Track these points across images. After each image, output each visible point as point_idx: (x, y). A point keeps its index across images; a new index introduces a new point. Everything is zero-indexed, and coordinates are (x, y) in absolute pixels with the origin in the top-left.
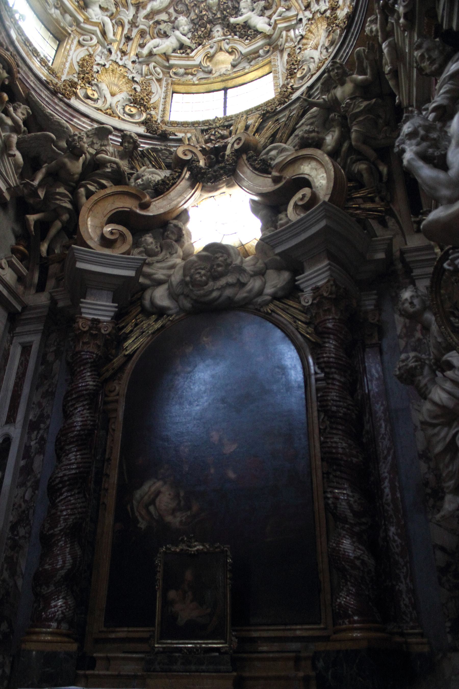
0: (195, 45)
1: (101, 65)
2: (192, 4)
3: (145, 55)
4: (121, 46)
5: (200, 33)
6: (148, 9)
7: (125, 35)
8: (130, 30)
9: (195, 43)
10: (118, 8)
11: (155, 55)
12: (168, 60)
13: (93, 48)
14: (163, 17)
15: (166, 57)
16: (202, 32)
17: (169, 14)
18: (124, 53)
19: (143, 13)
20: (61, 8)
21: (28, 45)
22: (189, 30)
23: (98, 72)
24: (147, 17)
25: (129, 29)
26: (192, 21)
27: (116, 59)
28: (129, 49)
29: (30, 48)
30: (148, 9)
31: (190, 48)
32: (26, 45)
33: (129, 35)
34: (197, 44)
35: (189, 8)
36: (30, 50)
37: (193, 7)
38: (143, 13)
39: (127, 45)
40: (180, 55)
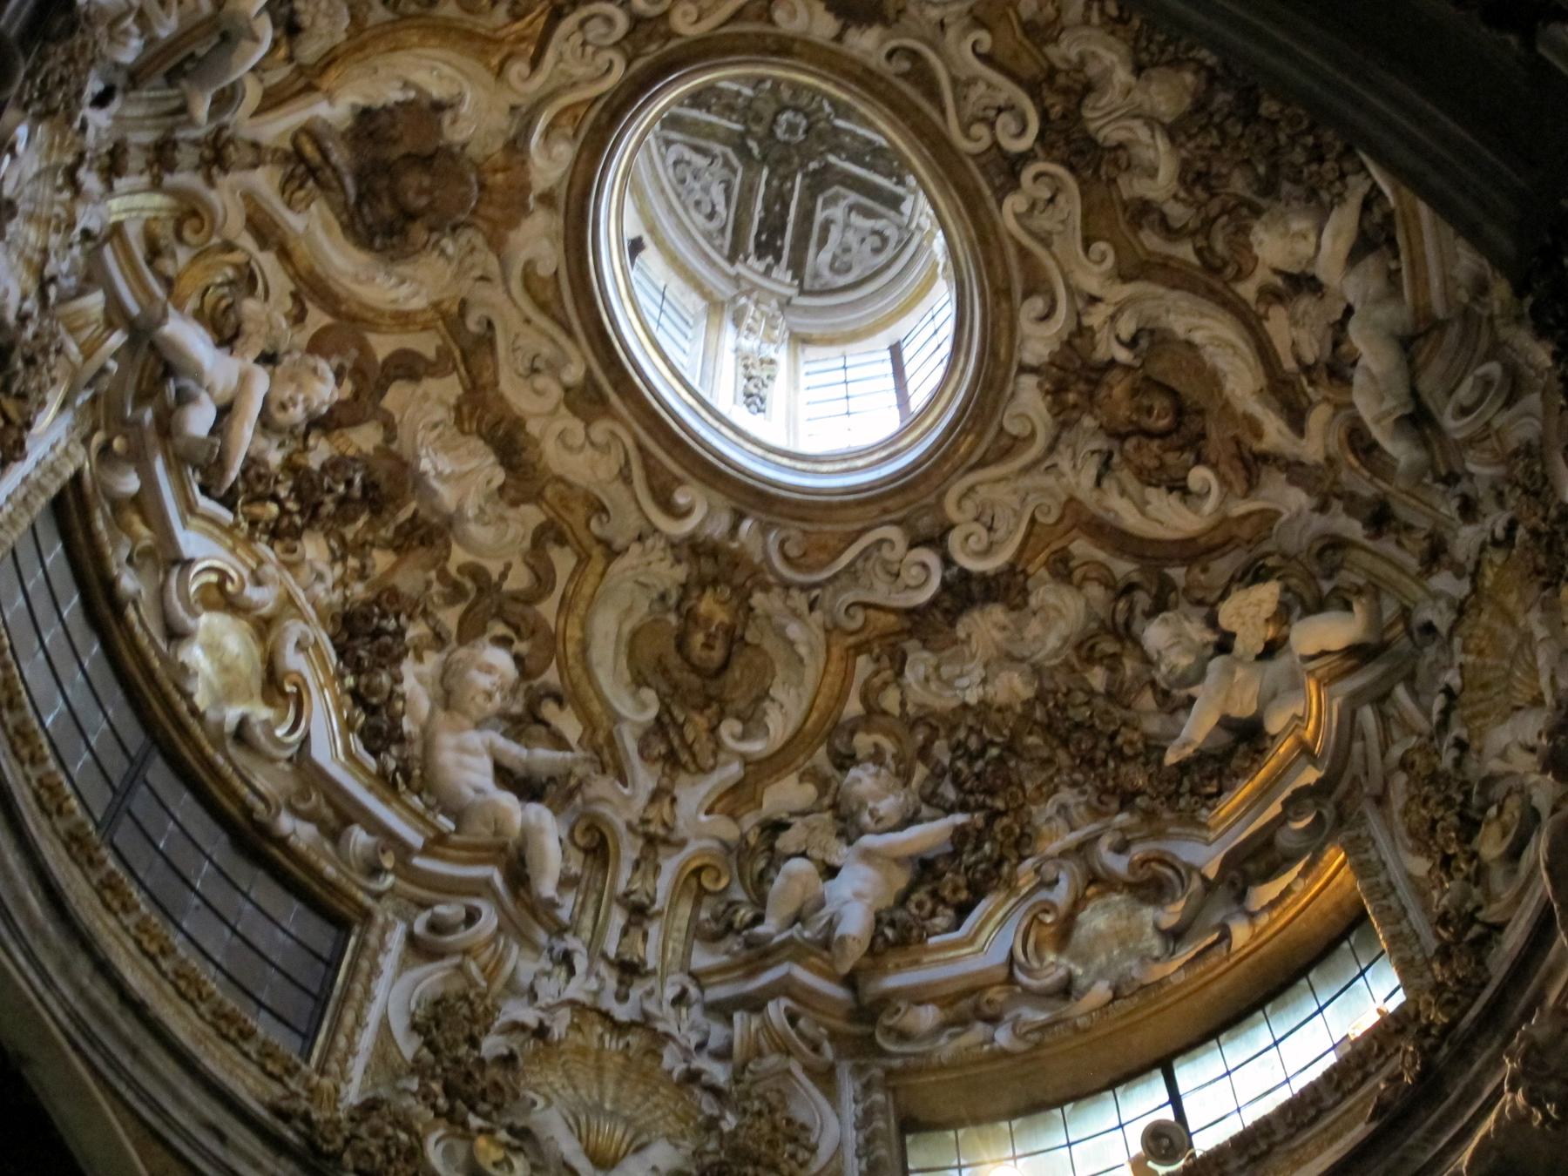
0: (1352, 180)
1: (1446, 712)
2: (1200, 193)
3: (1419, 456)
4: (1413, 564)
5: (1298, 156)
6: (1256, 409)
7: (1369, 537)
8: (1352, 503)
9: (1343, 176)
10: (1271, 562)
11: (1414, 394)
12: (1439, 326)
13: (1396, 733)
14: (1278, 325)
15: (1426, 334)
16: (1293, 139)
17: (1270, 295)
18: (1435, 554)
19: (1274, 432)
20: (1251, 867)
21: (1263, 1146)
22: (1308, 200)
23: (1461, 745)
24: (1296, 419)
25: (1350, 512)
26: (1268, 188)
27: (1451, 605)
28: (1423, 524)
29: (1279, 1137)
30: (1256, 409)
31: (1366, 205)
32: (1267, 1154)
33: (1368, 512)
34: (1347, 166)
35: (1214, 207)
36: (1290, 1138)
37: (1208, 188)
38: (1274, 432)
39: (1409, 528)
40: (1403, 257)
